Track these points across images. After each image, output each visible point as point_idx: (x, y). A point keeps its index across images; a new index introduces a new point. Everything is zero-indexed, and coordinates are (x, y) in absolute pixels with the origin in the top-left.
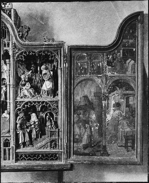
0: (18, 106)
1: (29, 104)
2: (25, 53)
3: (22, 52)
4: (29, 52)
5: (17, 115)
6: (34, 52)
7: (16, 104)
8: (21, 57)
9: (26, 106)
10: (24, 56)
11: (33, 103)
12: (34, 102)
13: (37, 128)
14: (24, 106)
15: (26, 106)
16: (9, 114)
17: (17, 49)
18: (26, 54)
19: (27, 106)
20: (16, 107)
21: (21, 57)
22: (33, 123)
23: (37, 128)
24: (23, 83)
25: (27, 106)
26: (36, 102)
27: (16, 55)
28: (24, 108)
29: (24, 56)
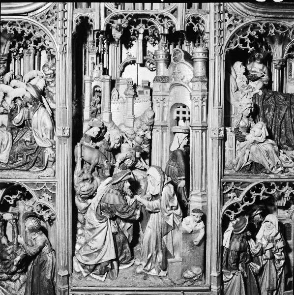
0: (232, 195)
1: (264, 189)
2: (254, 27)
3: (245, 28)
4: (267, 27)
5: (224, 223)
6: (284, 28)
7: (224, 188)
8: (242, 41)
9: (254, 195)
10: (250, 37)
11: (276, 188)
12: (277, 183)
13: (279, 260)
14: (248, 197)
15: (254, 195)
16: (204, 219)
17: (230, 16)
18: (258, 33)
19: (258, 197)
20: (224, 199)
21: (242, 41)
22: (270, 245)
23: (279, 260)
24: (244, 123)
25: (258, 197)
26: (284, 184)
27: (228, 35)
28: (247, 203)
29: (250, 37)
